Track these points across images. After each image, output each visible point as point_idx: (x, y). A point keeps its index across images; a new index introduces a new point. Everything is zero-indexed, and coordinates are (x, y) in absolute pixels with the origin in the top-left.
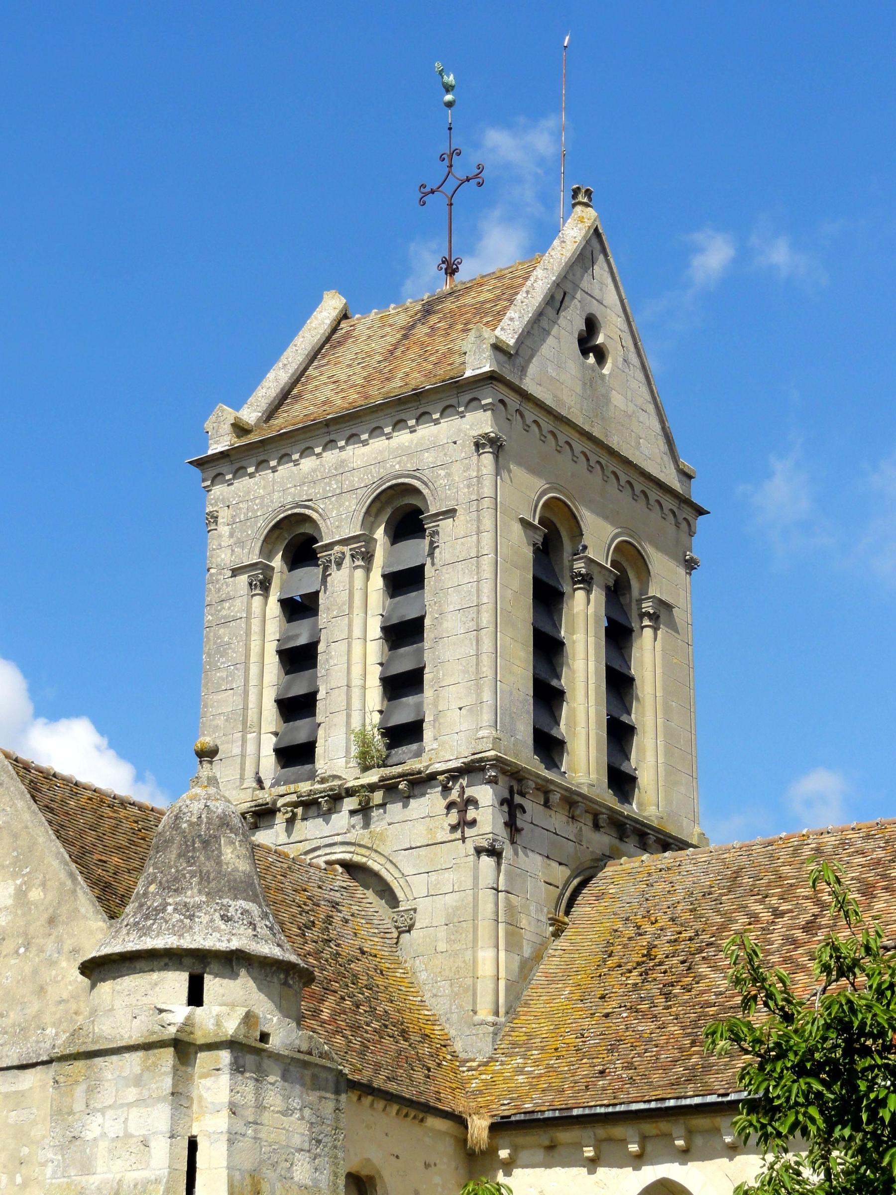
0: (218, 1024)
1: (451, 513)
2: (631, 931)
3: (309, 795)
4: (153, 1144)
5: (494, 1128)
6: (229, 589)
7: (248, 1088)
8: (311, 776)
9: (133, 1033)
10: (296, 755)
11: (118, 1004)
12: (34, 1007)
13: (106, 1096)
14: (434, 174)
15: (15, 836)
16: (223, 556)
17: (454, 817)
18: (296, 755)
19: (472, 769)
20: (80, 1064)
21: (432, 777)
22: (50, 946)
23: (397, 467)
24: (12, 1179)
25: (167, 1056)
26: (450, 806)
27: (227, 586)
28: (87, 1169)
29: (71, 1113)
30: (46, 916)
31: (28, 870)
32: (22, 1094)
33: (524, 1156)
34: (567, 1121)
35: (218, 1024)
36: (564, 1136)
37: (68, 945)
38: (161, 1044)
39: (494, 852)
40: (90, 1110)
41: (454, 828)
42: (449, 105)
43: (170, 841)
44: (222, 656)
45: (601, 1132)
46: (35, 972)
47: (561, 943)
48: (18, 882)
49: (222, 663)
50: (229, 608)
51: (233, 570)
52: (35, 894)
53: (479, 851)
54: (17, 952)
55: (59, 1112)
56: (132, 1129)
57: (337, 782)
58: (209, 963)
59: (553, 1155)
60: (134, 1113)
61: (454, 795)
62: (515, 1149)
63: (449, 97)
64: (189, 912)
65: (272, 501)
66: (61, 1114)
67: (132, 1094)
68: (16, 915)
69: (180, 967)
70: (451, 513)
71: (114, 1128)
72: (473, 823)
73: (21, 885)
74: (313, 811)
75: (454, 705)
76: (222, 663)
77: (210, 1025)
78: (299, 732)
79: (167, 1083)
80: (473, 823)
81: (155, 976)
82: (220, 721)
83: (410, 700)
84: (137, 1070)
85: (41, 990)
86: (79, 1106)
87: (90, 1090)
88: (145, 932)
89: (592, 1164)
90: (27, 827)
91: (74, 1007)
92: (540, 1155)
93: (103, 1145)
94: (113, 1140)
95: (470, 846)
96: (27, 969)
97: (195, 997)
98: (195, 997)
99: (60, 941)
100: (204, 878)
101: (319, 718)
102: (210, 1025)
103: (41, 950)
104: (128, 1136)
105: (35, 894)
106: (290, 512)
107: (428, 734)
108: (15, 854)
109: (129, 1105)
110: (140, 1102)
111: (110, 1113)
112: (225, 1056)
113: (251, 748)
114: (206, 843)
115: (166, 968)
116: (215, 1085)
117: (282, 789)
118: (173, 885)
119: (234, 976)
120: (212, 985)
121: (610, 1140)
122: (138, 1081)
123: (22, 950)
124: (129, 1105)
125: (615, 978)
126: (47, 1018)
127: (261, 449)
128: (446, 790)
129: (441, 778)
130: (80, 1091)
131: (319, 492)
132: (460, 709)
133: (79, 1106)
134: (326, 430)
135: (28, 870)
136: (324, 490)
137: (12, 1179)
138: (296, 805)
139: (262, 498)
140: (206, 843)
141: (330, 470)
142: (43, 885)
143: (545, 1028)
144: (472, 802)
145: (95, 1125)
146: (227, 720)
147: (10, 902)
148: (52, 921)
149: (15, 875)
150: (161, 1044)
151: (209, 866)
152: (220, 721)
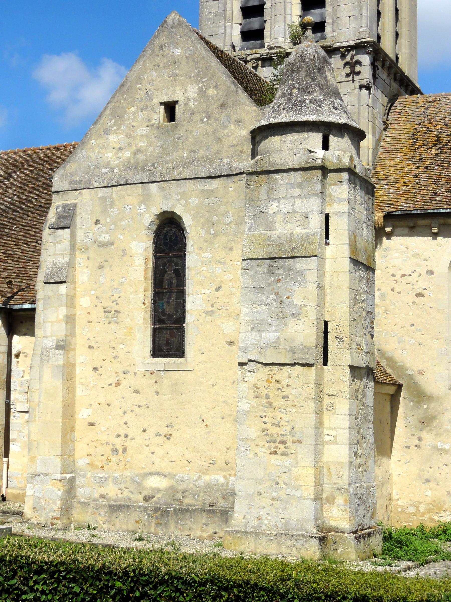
0: (339, 159)
2: (424, 130)
3: (267, 55)
4: (310, 217)
5: (385, 217)
7: (352, 191)
8: (262, 46)
9: (296, 162)
10: (252, 35)
11: (284, 147)
12: (215, 148)
13: (281, 192)
15: (197, 62)
17: (348, 70)
18: (252, 35)
19: (359, 47)
20: (263, 176)
21: (338, 49)
22: (223, 118)
24: (208, 232)
25: (319, 173)
26: (346, 64)
28: (270, 226)
29: (259, 200)
30: (219, 103)
31: (206, 79)
32: (212, 191)
33: (397, 230)
34: (424, 215)
35: (339, 159)
36: (422, 222)
37: (234, 118)
38: (315, 168)
39: (368, 88)
40: (270, 199)
41: (347, 75)
43: (301, 67)
45: (442, 221)
46: (215, 131)
47: (387, 133)
48: (200, 85)
52: (211, 92)
53: (361, 87)
54: (202, 120)
55: (251, 199)
56: (297, 208)
57: (279, 50)
58: (332, 130)
59: (413, 230)
60: (298, 201)
61: (348, 59)
62: (394, 227)
64: (318, 104)
66: (251, 200)
67: (296, 192)
68: (201, 102)
69: (318, 131)
71: (285, 208)
72: (358, 73)
73: (202, 87)
74: (267, 63)
75: (346, 15)
77: (335, 160)
78: (255, 23)
79: (319, 187)
80: (358, 73)
81: (306, 134)
82: (212, 16)
83: (317, 11)
84: (299, 180)
85: (219, 140)
86: (263, 196)
87: (270, 190)
88: (298, 112)
89: (435, 236)
90: (204, 57)
91: (240, 149)
92: (406, 230)
93: (279, 216)
94: (286, 214)
95: (357, 84)
96: (210, 129)
97: (326, 147)
98: (326, 147)
99: (229, 116)
100: (321, 88)
101: (265, 18)
102: (335, 160)
103: (217, 120)
104: (294, 212)
105: (211, 92)
107: (328, 28)
108: (197, 71)
109: (295, 197)
110: (300, 196)
111: (282, 201)
112: (345, 176)
113: (228, 31)
114: (319, 70)
115: (311, 130)
116: (341, 189)
117: (248, 52)
118: (306, 90)
119: (342, 137)
120: (333, 140)
121: (444, 225)
122: (300, 186)
123: (205, 120)
124: (295, 197)
125: (423, 151)
126: (224, 154)
128: (343, 56)
129: (342, 50)
130: (263, 190)
132: (349, 17)
133: (263, 196)
135: (206, 79)
137: (209, 232)
138: (258, 59)
140: (319, 70)
142: (216, 87)
143: (394, 172)
144: (359, 63)
145: (274, 206)
146: (215, 16)
147: (196, 95)
148: (223, 106)
149: (197, 82)
150: (315, 168)
151: (322, 81)
152: (212, 16)
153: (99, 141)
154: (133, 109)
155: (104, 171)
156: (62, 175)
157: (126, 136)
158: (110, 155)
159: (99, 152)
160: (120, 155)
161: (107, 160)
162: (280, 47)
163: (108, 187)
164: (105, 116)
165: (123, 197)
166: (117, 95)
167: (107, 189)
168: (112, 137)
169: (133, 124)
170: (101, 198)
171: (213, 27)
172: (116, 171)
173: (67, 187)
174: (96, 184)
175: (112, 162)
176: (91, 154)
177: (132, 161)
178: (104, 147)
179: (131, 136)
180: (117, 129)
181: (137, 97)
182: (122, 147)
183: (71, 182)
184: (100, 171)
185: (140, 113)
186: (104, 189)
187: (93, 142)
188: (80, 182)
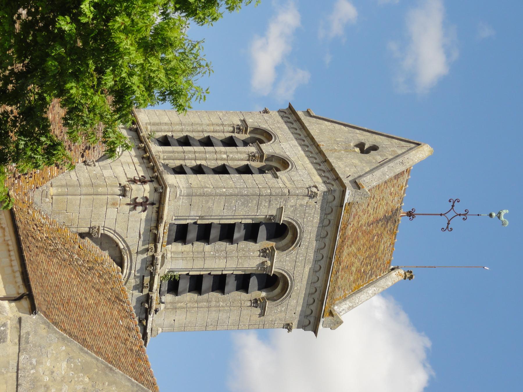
1: (262, 314)
6: (274, 205)
14: (456, 223)
16: (292, 201)
23: (296, 288)
27: (276, 204)
42: (491, 215)
44: (242, 202)
49: (239, 203)
50: (265, 206)
51: (282, 208)
63: (494, 215)
65: (308, 227)
70: (262, 314)
76: (239, 203)
82: (210, 204)
106: (299, 235)
127: (335, 223)
131: (301, 250)
134: (329, 256)
136: (301, 253)
139: (312, 221)
141: (309, 256)
152: (210, 204)
153: (63, 353)
154: (87, 380)
155: (34, 361)
156: (37, 322)
157: (63, 377)
158: (48, 364)
159: (53, 354)
160: (47, 373)
161: (44, 361)
162: (162, 265)
163: (18, 369)
164: (85, 357)
165: (6, 383)
166: (103, 366)
167: (16, 368)
168: (64, 364)
169: (73, 382)
170: (8, 362)
171: (199, 206)
172: (32, 372)
173: (23, 332)
174: (22, 358)
175: (41, 366)
176: (52, 347)
177: (39, 384)
178: (56, 358)
179: (62, 381)
180: (71, 368)
181: (97, 383)
182: (54, 374)
183: (28, 333)
184: (34, 357)
185: (82, 387)
186: (16, 365)
187: (64, 348)
188: (27, 342)
